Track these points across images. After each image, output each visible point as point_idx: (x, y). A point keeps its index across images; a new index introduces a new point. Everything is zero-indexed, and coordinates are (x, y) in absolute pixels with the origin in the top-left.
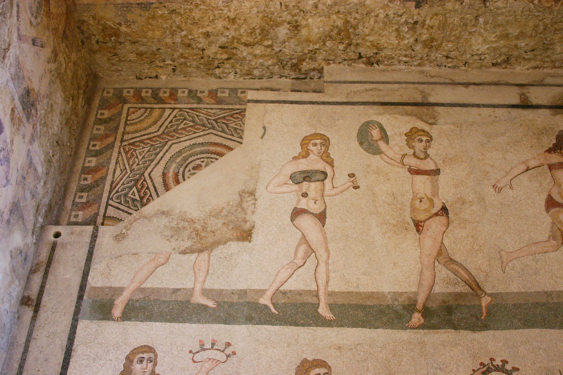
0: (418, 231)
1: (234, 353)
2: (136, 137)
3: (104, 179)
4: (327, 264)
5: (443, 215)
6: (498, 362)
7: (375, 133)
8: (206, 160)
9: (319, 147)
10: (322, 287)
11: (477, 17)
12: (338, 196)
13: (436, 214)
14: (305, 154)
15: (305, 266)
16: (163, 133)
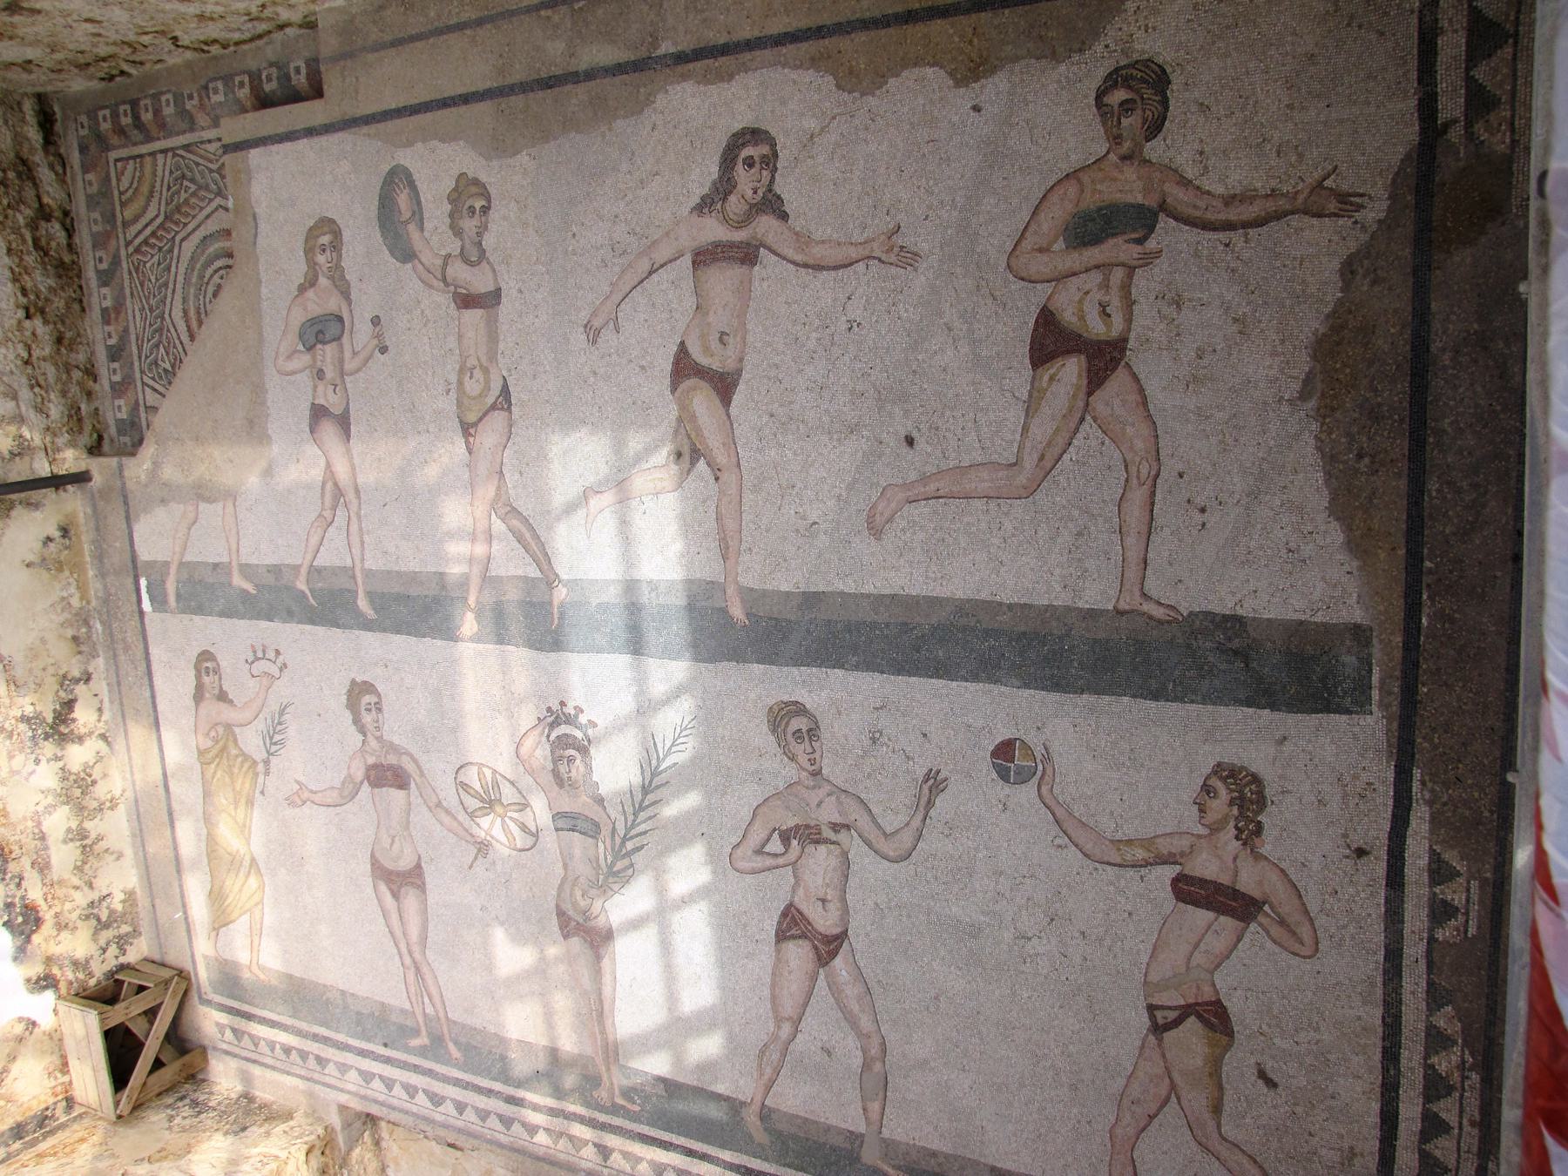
2: (140, 232)
3: (126, 330)
4: (359, 518)
5: (502, 409)
7: (403, 199)
8: (222, 272)
9: (328, 252)
10: (358, 562)
12: (361, 374)
13: (493, 407)
15: (335, 524)
16: (166, 217)
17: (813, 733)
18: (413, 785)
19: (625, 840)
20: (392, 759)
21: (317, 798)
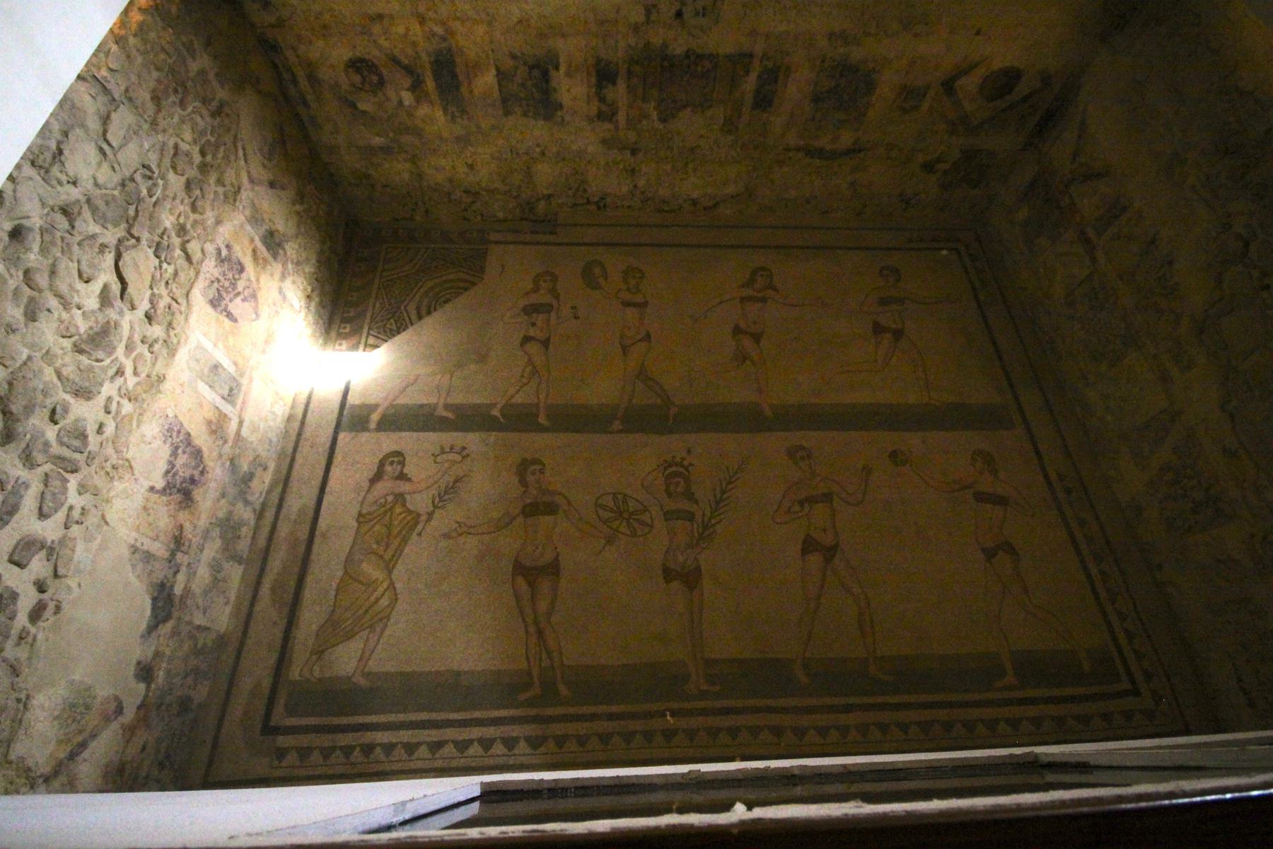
0: (624, 353)
1: (468, 455)
6: (678, 459)
7: (597, 271)
11: (686, 164)
13: (640, 340)
14: (536, 289)
17: (809, 457)
18: (561, 512)
19: (710, 519)
20: (547, 498)
21: (472, 531)
